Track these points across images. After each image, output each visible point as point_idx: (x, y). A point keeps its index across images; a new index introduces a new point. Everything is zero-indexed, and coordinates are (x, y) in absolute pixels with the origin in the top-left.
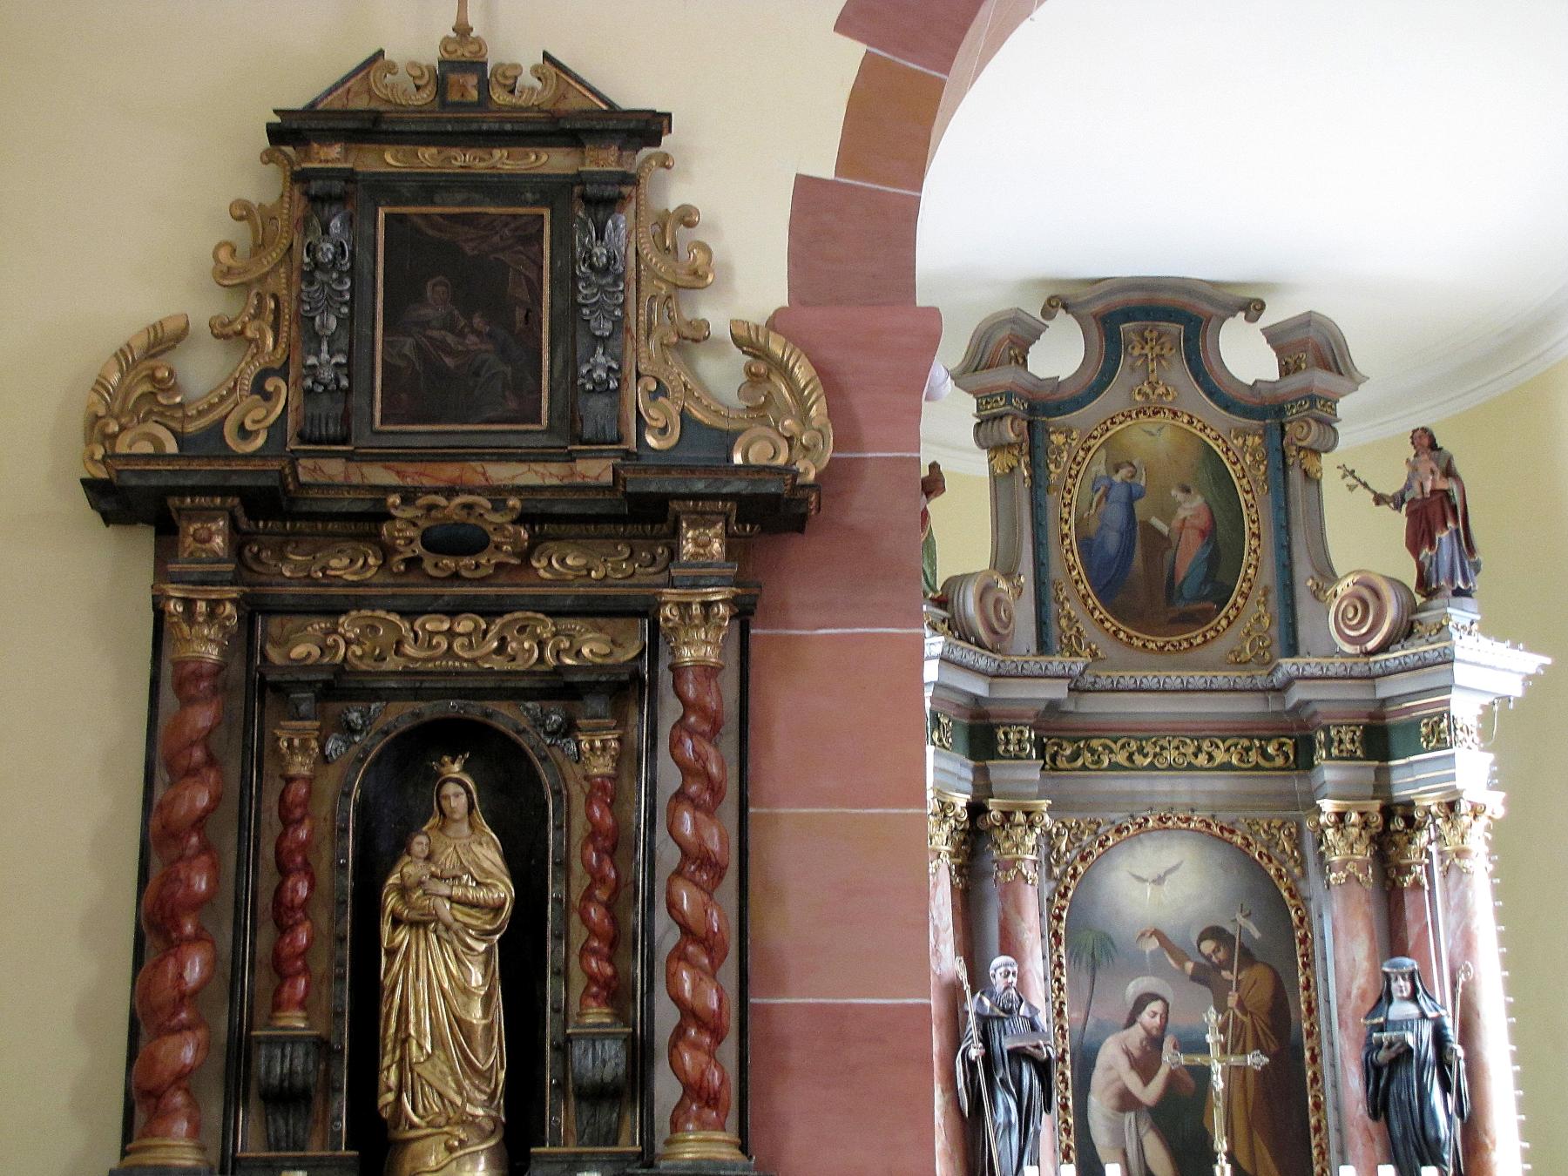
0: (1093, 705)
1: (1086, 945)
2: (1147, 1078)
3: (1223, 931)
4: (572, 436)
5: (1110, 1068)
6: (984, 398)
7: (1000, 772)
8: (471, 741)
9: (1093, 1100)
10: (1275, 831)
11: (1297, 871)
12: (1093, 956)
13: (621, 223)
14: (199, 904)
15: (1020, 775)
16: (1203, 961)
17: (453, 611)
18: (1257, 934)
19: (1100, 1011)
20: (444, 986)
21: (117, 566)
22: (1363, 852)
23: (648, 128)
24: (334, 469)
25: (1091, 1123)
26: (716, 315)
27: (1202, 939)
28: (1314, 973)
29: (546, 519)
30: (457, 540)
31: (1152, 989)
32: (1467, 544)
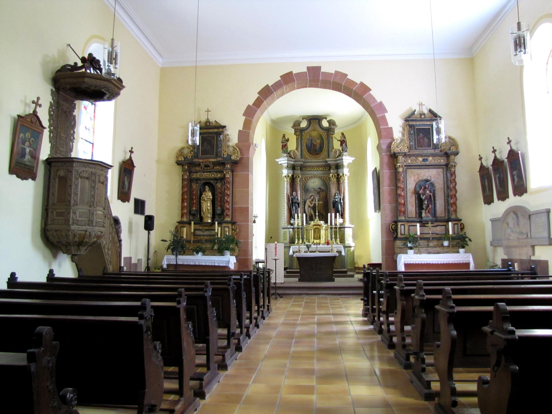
0: (307, 164)
1: (305, 190)
4: (217, 156)
6: (295, 130)
7: (295, 172)
8: (210, 184)
13: (221, 136)
14: (186, 199)
15: (298, 172)
17: (207, 172)
20: (207, 206)
21: (179, 168)
22: (335, 180)
23: (225, 127)
24: (197, 160)
26: (231, 144)
29: (215, 164)
30: (207, 166)
32: (346, 146)
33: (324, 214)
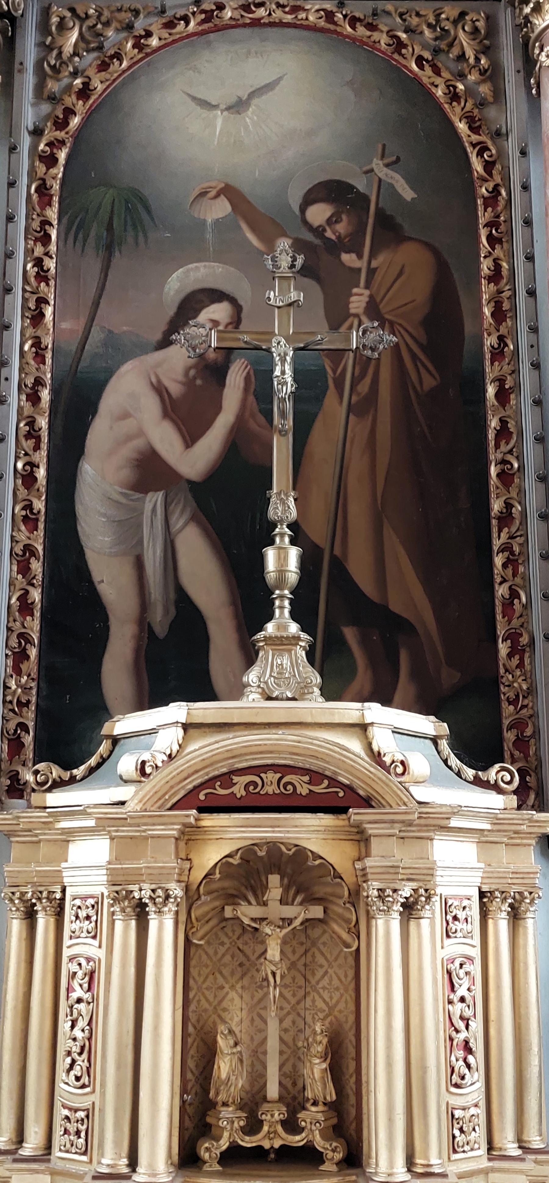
3: (351, 188)
5: (125, 415)
9: (89, 471)
10: (448, 26)
11: (485, 89)
12: (110, 228)
16: (309, 237)
18: (408, 194)
19: (114, 318)
25: (80, 509)
27: (308, 200)
33: (408, 595)
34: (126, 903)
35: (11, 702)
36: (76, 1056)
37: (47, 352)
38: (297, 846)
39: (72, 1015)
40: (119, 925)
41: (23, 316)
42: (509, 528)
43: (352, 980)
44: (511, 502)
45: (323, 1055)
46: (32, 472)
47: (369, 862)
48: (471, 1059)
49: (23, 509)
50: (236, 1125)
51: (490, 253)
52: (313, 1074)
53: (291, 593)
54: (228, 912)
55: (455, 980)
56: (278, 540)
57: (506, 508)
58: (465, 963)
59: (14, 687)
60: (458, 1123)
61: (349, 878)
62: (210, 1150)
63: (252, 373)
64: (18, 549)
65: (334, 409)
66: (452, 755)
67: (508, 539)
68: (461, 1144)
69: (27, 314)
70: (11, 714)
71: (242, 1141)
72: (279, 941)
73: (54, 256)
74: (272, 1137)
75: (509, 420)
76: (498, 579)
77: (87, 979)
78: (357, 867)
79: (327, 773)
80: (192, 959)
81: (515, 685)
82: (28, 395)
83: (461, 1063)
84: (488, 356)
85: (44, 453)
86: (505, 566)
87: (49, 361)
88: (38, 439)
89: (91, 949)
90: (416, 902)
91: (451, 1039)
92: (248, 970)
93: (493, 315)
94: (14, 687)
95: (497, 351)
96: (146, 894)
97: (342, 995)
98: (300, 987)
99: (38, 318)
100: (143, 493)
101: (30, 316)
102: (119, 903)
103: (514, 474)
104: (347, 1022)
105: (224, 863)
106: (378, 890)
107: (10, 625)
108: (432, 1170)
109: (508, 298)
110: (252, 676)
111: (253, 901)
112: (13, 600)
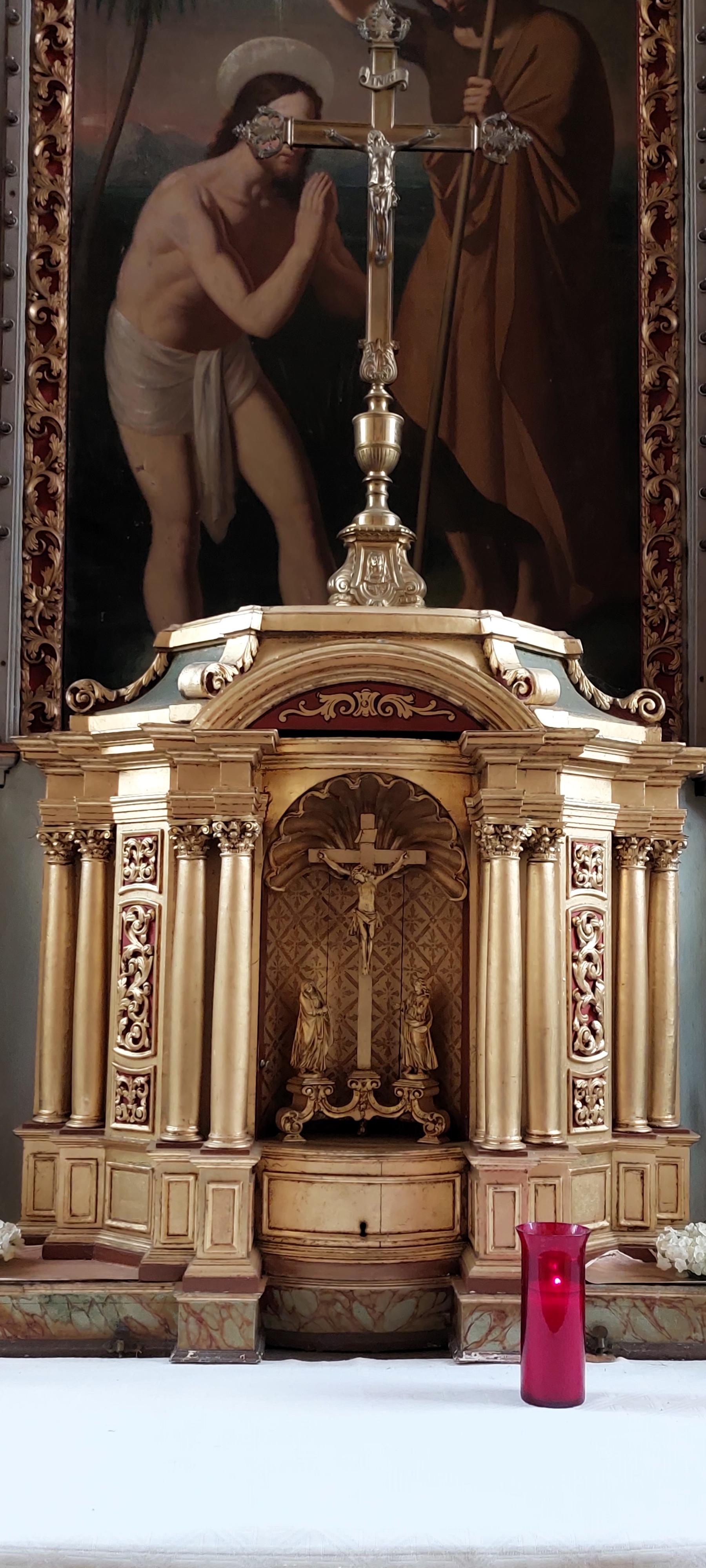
2: (253, 277)
5: (168, 247)
9: (122, 321)
25: (111, 373)
28: (679, 38)
31: (277, 67)
34: (193, 840)
35: (31, 619)
36: (133, 1016)
37: (64, 158)
38: (396, 778)
39: (127, 971)
40: (184, 865)
41: (32, 107)
42: (662, 407)
43: (459, 933)
44: (667, 371)
45: (424, 1018)
46: (49, 321)
47: (484, 794)
48: (597, 1024)
49: (39, 370)
50: (321, 1093)
51: (651, 30)
52: (412, 1039)
53: (389, 475)
54: (313, 856)
55: (582, 936)
56: (372, 405)
57: (660, 379)
58: (593, 917)
59: (34, 600)
60: (580, 1094)
61: (458, 817)
62: (291, 1121)
63: (334, 192)
64: (34, 423)
65: (442, 243)
66: (585, 678)
67: (661, 420)
68: (582, 1116)
69: (36, 105)
70: (32, 633)
71: (329, 1111)
72: (373, 890)
73: (71, 24)
74: (362, 1108)
75: (667, 262)
76: (646, 473)
77: (144, 929)
78: (468, 804)
79: (436, 692)
80: (270, 908)
81: (661, 606)
82: (40, 217)
83: (585, 1028)
84: (644, 174)
85: (64, 296)
86: (655, 455)
87: (67, 170)
88: (56, 277)
89: (149, 894)
90: (539, 843)
91: (575, 1001)
92: (335, 925)
93: (652, 117)
94: (34, 600)
95: (656, 168)
96: (218, 826)
97: (446, 953)
98: (397, 945)
99: (51, 111)
100: (192, 352)
101: (41, 108)
102: (184, 840)
103: (671, 335)
104: (451, 981)
105: (309, 796)
106: (495, 826)
107: (27, 521)
108: (550, 1141)
109: (673, 95)
110: (339, 581)
111: (341, 844)
112: (30, 489)
